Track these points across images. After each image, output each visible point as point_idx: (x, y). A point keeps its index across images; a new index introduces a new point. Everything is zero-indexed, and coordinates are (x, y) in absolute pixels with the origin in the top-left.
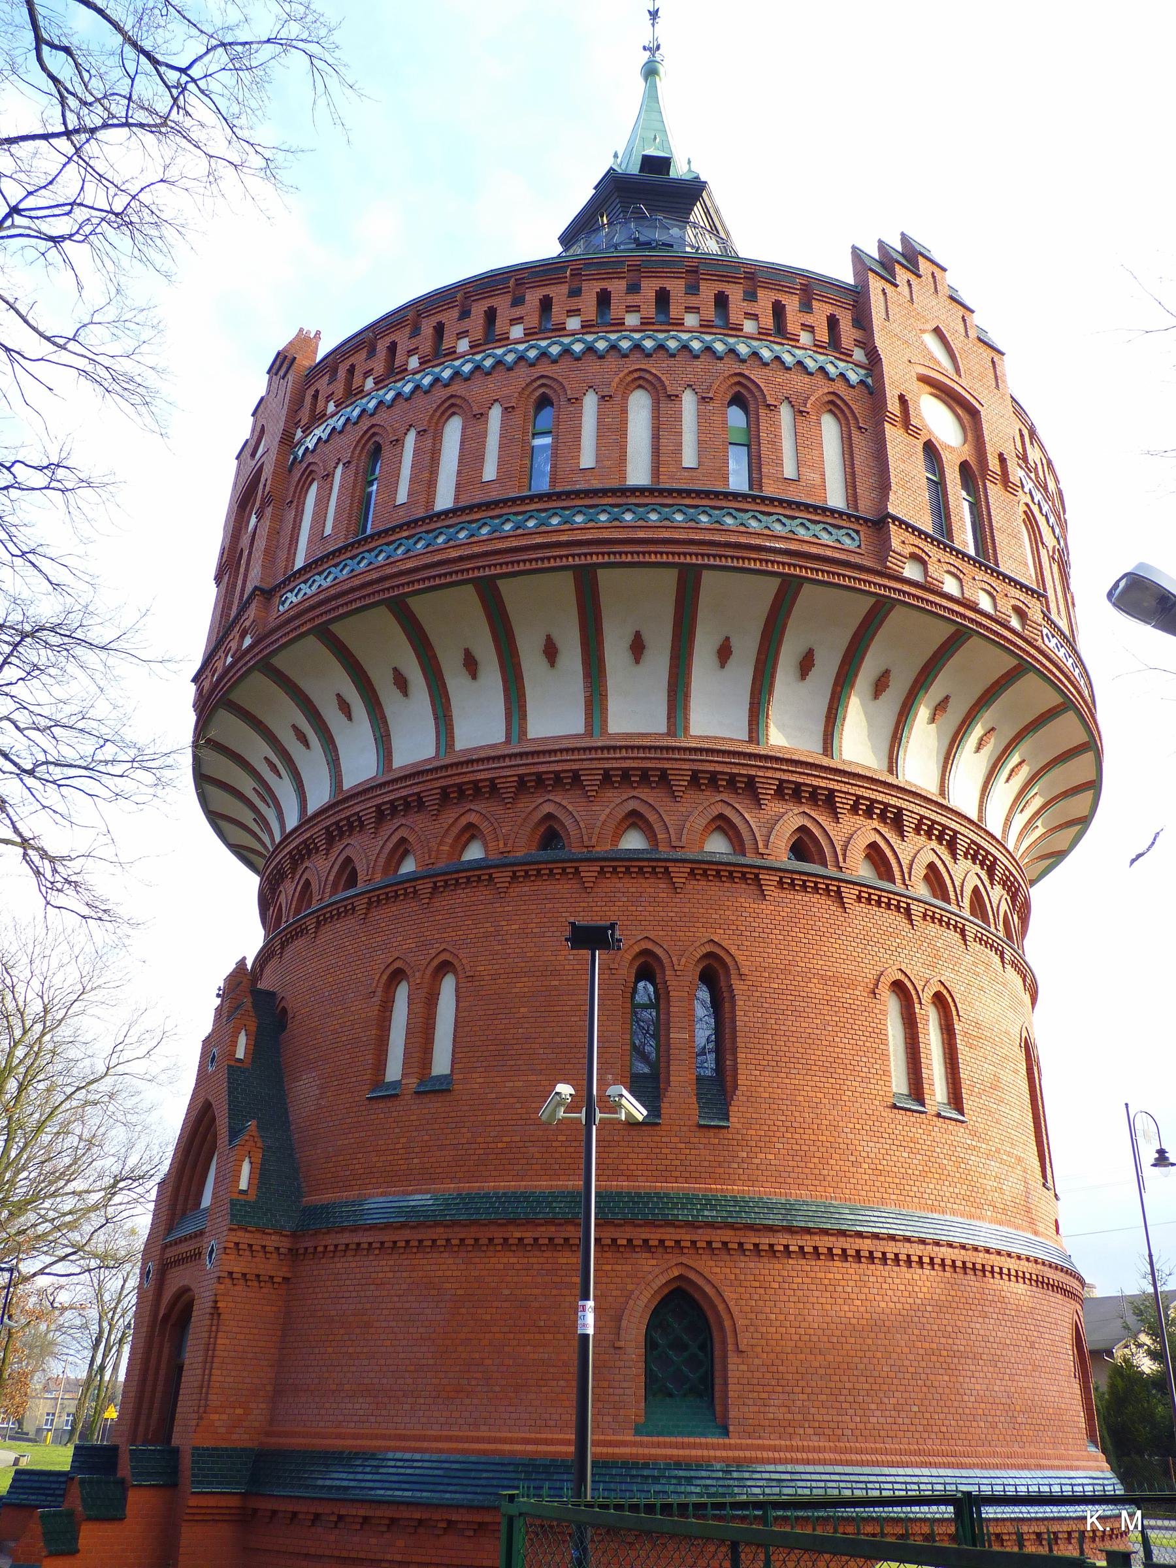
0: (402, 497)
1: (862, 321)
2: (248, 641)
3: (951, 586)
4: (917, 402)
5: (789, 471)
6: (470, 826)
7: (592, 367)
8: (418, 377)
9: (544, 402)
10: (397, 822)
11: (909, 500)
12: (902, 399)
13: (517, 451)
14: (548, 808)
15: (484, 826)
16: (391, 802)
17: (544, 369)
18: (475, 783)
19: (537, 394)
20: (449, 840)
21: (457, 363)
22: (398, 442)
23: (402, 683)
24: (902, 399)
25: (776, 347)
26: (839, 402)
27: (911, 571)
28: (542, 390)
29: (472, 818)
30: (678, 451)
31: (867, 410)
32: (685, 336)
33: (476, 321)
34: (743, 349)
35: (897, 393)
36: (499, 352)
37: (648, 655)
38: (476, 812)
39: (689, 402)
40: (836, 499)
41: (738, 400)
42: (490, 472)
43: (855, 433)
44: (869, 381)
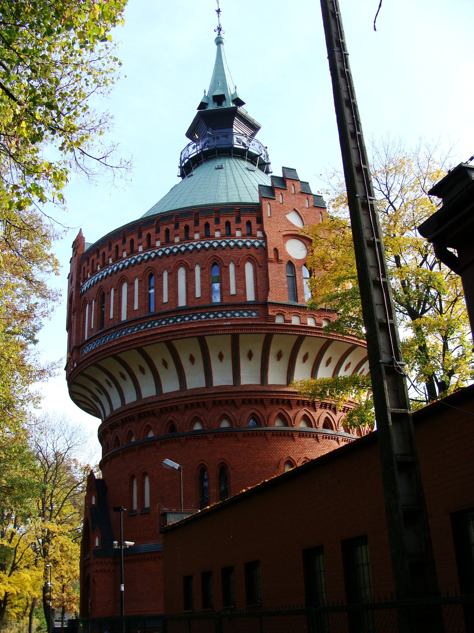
0: (111, 317)
1: (260, 221)
2: (75, 365)
3: (295, 321)
4: (284, 248)
6: (148, 426)
7: (166, 261)
8: (112, 267)
9: (151, 276)
11: (278, 294)
12: (276, 250)
13: (145, 297)
14: (170, 418)
16: (125, 418)
17: (150, 263)
19: (149, 273)
20: (143, 431)
21: (124, 262)
22: (109, 293)
24: (276, 250)
26: (252, 257)
27: (279, 320)
28: (150, 271)
29: (149, 423)
31: (262, 258)
32: (195, 243)
33: (128, 245)
35: (272, 248)
36: (136, 257)
37: (196, 361)
39: (197, 269)
41: (215, 264)
42: (136, 307)
43: (258, 268)
44: (264, 244)
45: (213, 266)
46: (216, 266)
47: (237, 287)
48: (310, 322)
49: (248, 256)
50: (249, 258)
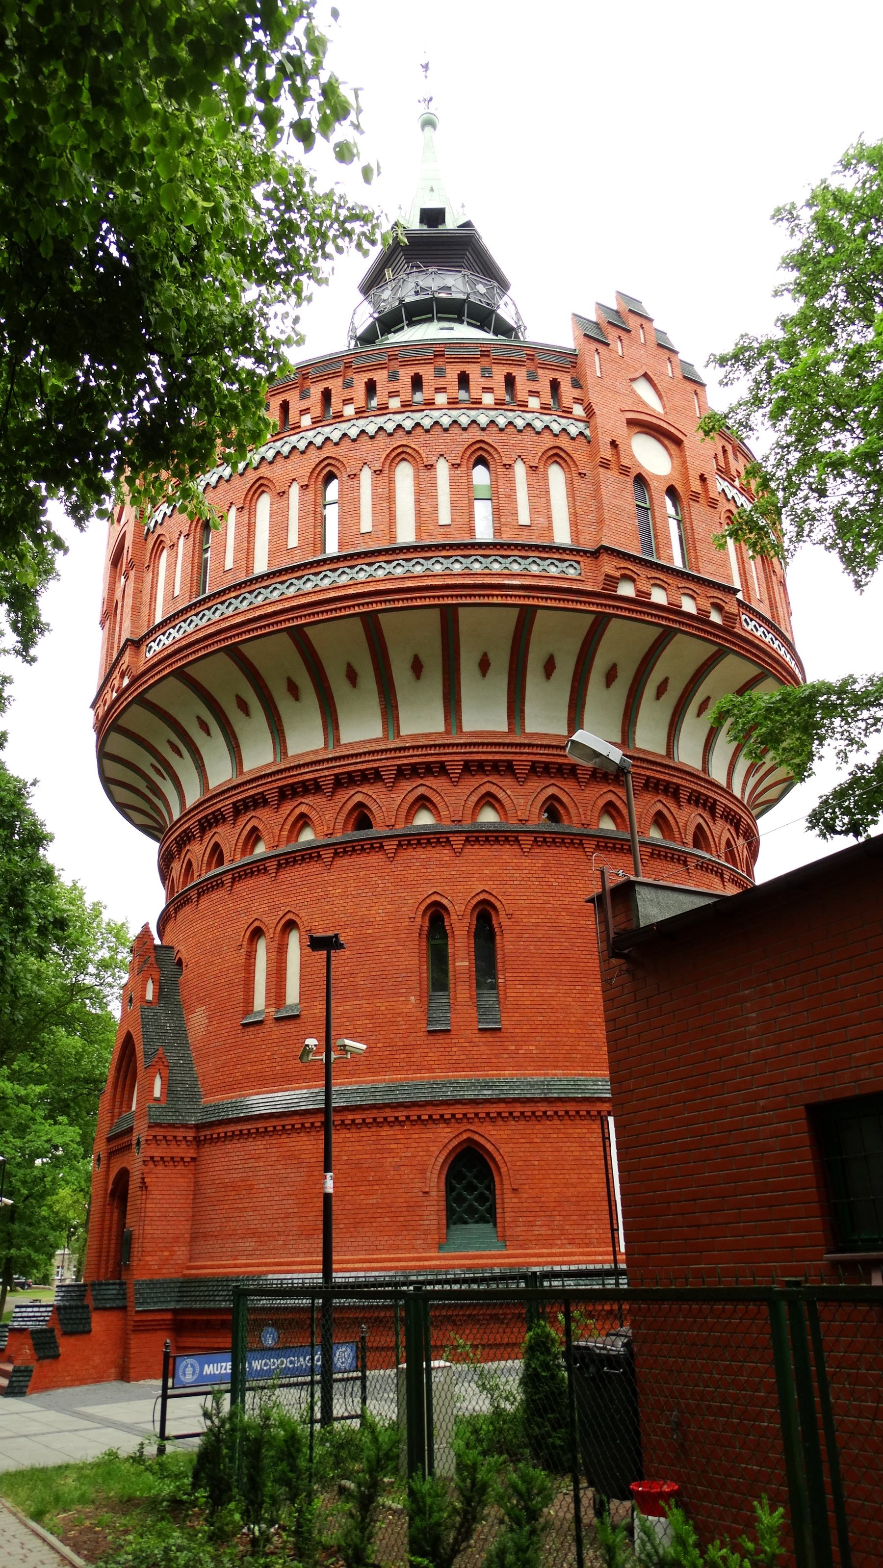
0: (229, 564)
2: (126, 681)
3: (659, 597)
5: (524, 518)
6: (303, 816)
9: (330, 477)
10: (250, 814)
14: (358, 798)
15: (313, 815)
18: (303, 782)
19: (325, 472)
23: (244, 707)
24: (614, 444)
25: (510, 414)
26: (562, 454)
29: (303, 809)
30: (435, 511)
34: (483, 420)
38: (306, 805)
40: (562, 536)
41: (481, 461)
42: (293, 541)
44: (587, 432)
45: (474, 466)
46: (480, 470)
47: (532, 511)
48: (689, 606)
49: (555, 451)
50: (556, 455)
